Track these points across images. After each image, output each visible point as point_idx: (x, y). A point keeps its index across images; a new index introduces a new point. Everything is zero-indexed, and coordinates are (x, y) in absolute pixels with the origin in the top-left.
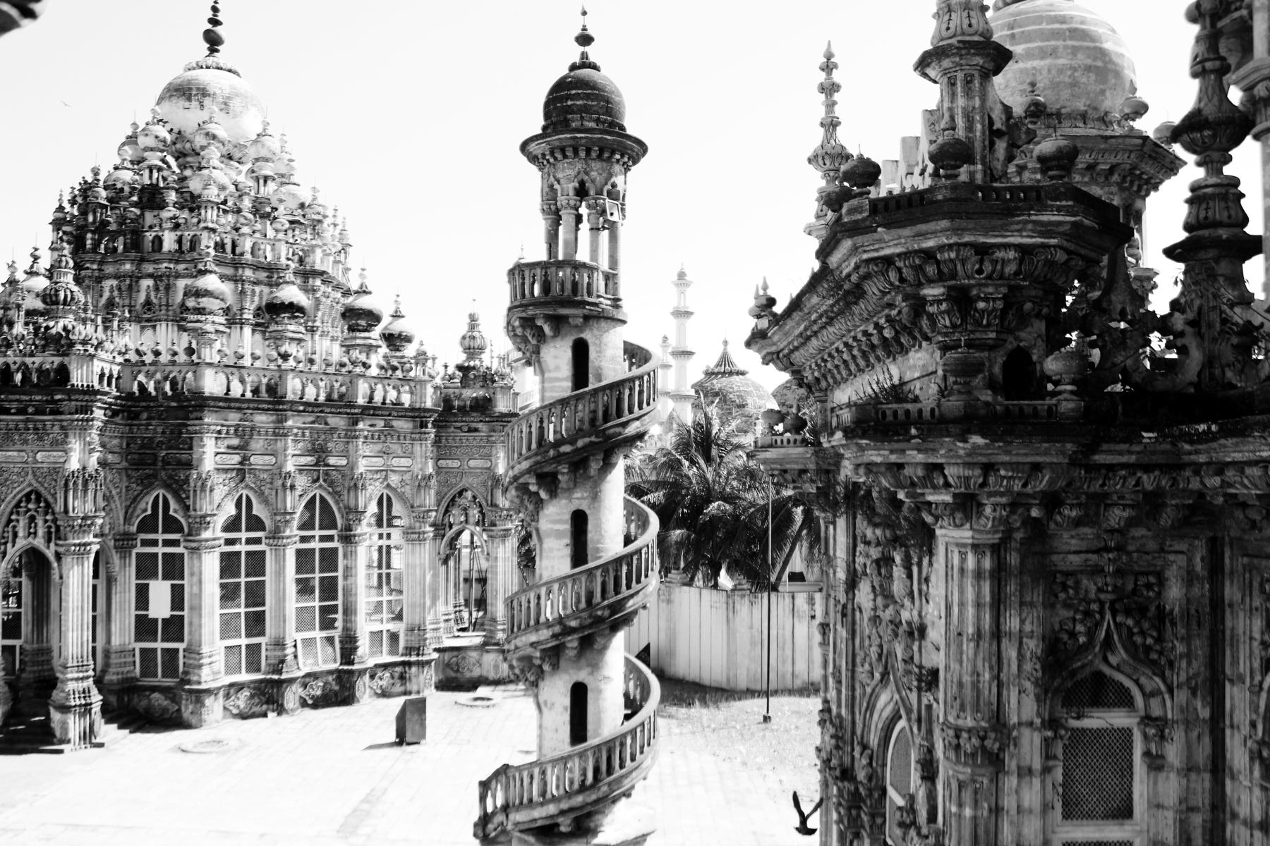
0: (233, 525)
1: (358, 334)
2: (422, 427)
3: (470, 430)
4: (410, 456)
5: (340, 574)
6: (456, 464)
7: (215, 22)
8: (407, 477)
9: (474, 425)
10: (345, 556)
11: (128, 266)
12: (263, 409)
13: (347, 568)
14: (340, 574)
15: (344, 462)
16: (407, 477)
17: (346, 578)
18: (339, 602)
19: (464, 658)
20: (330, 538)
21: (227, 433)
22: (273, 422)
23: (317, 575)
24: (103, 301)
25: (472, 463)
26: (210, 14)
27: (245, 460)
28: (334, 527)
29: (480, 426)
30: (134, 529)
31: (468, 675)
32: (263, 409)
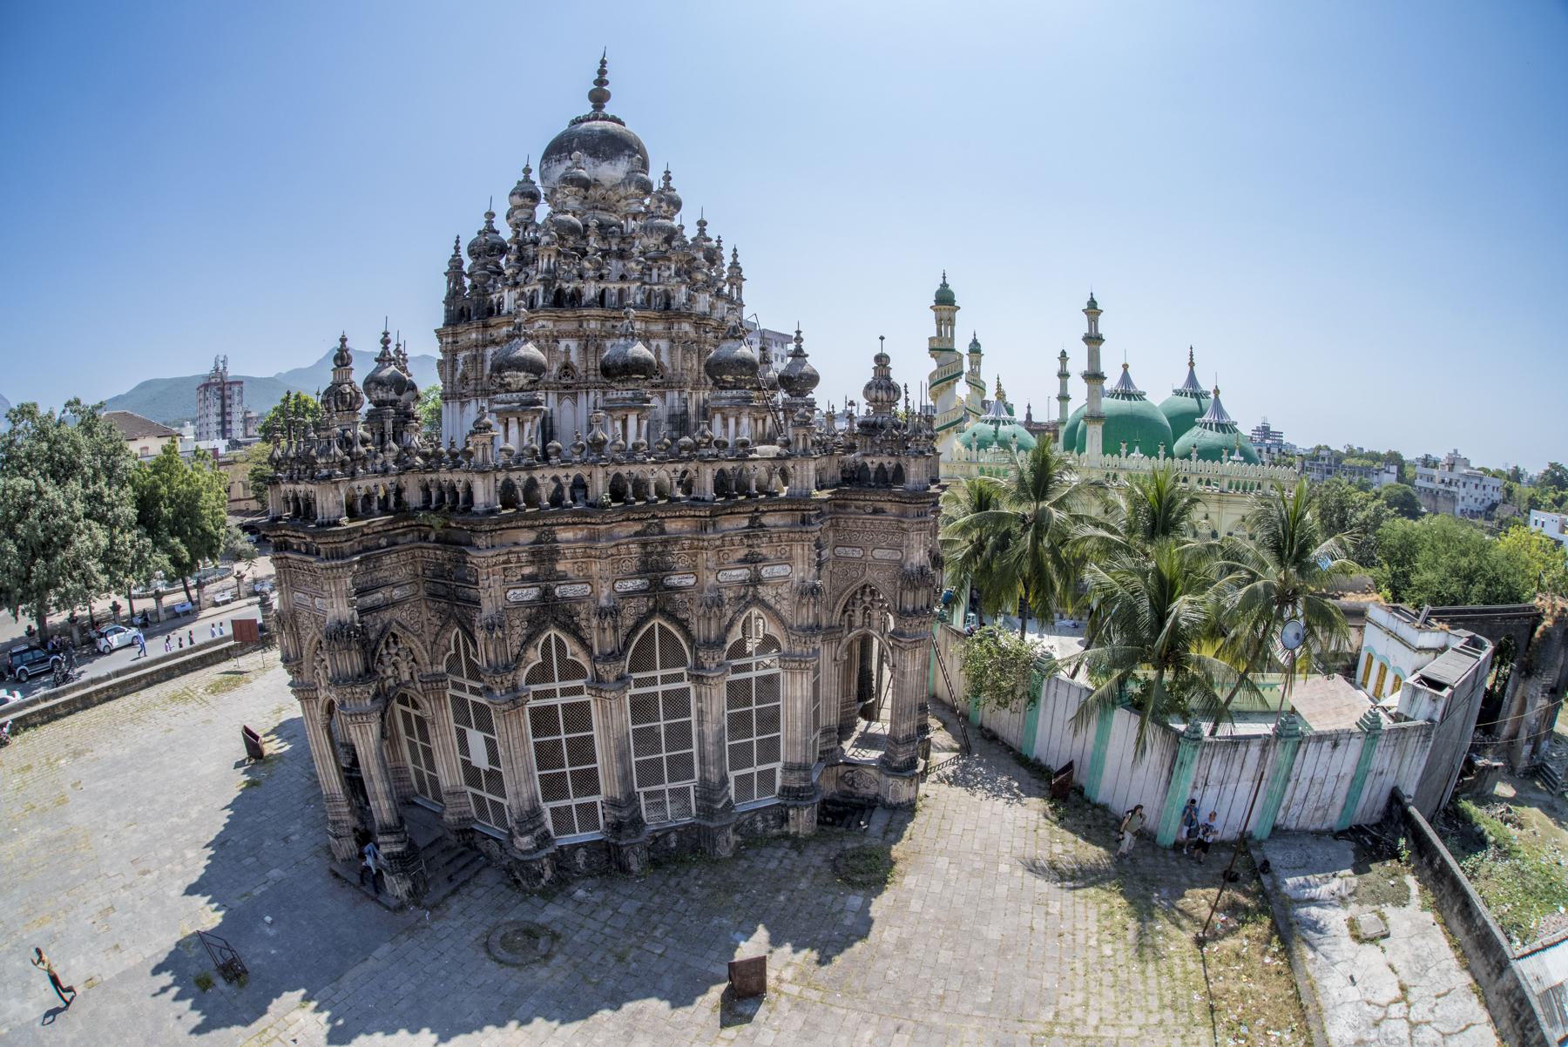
0: (541, 673)
1: (724, 393)
2: (803, 522)
3: (876, 511)
4: (789, 560)
5: (693, 718)
6: (858, 553)
7: (601, 82)
8: (784, 590)
9: (879, 505)
10: (699, 697)
11: (474, 336)
12: (567, 524)
13: (701, 712)
14: (693, 718)
15: (691, 581)
16: (784, 590)
17: (701, 722)
18: (695, 750)
19: (860, 774)
20: (679, 678)
21: (519, 560)
22: (585, 539)
23: (662, 723)
24: (458, 375)
25: (878, 554)
26: (596, 76)
27: (547, 593)
28: (684, 663)
29: (887, 506)
30: (443, 668)
31: (863, 791)
32: (567, 524)
